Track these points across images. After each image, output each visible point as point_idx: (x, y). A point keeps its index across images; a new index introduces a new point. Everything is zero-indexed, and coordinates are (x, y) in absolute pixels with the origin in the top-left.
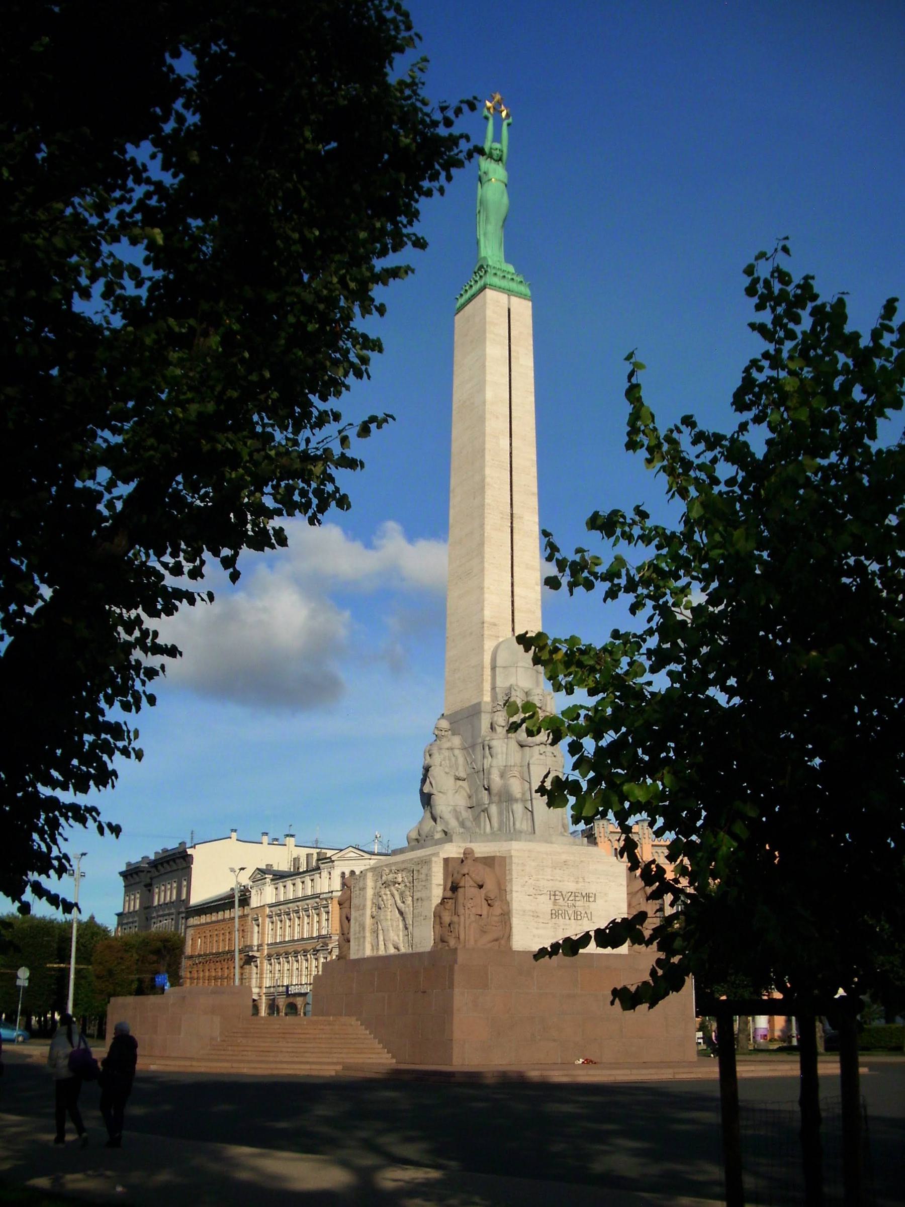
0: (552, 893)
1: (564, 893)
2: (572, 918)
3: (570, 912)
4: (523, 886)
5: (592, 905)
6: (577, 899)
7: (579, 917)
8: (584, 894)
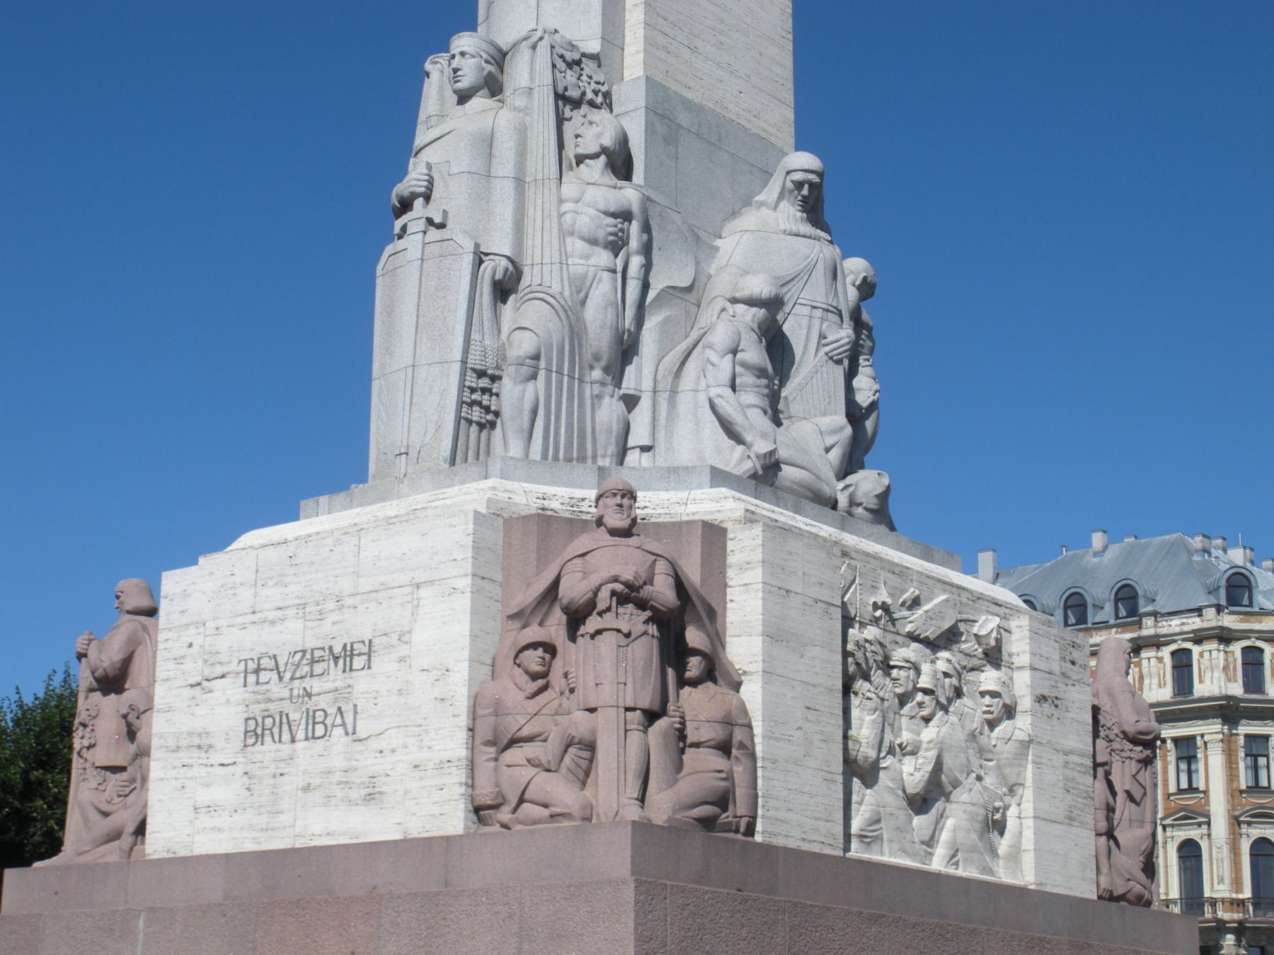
0: (252, 666)
1: (282, 662)
2: (300, 735)
3: (294, 716)
4: (179, 660)
5: (362, 683)
6: (318, 669)
7: (320, 730)
8: (337, 649)
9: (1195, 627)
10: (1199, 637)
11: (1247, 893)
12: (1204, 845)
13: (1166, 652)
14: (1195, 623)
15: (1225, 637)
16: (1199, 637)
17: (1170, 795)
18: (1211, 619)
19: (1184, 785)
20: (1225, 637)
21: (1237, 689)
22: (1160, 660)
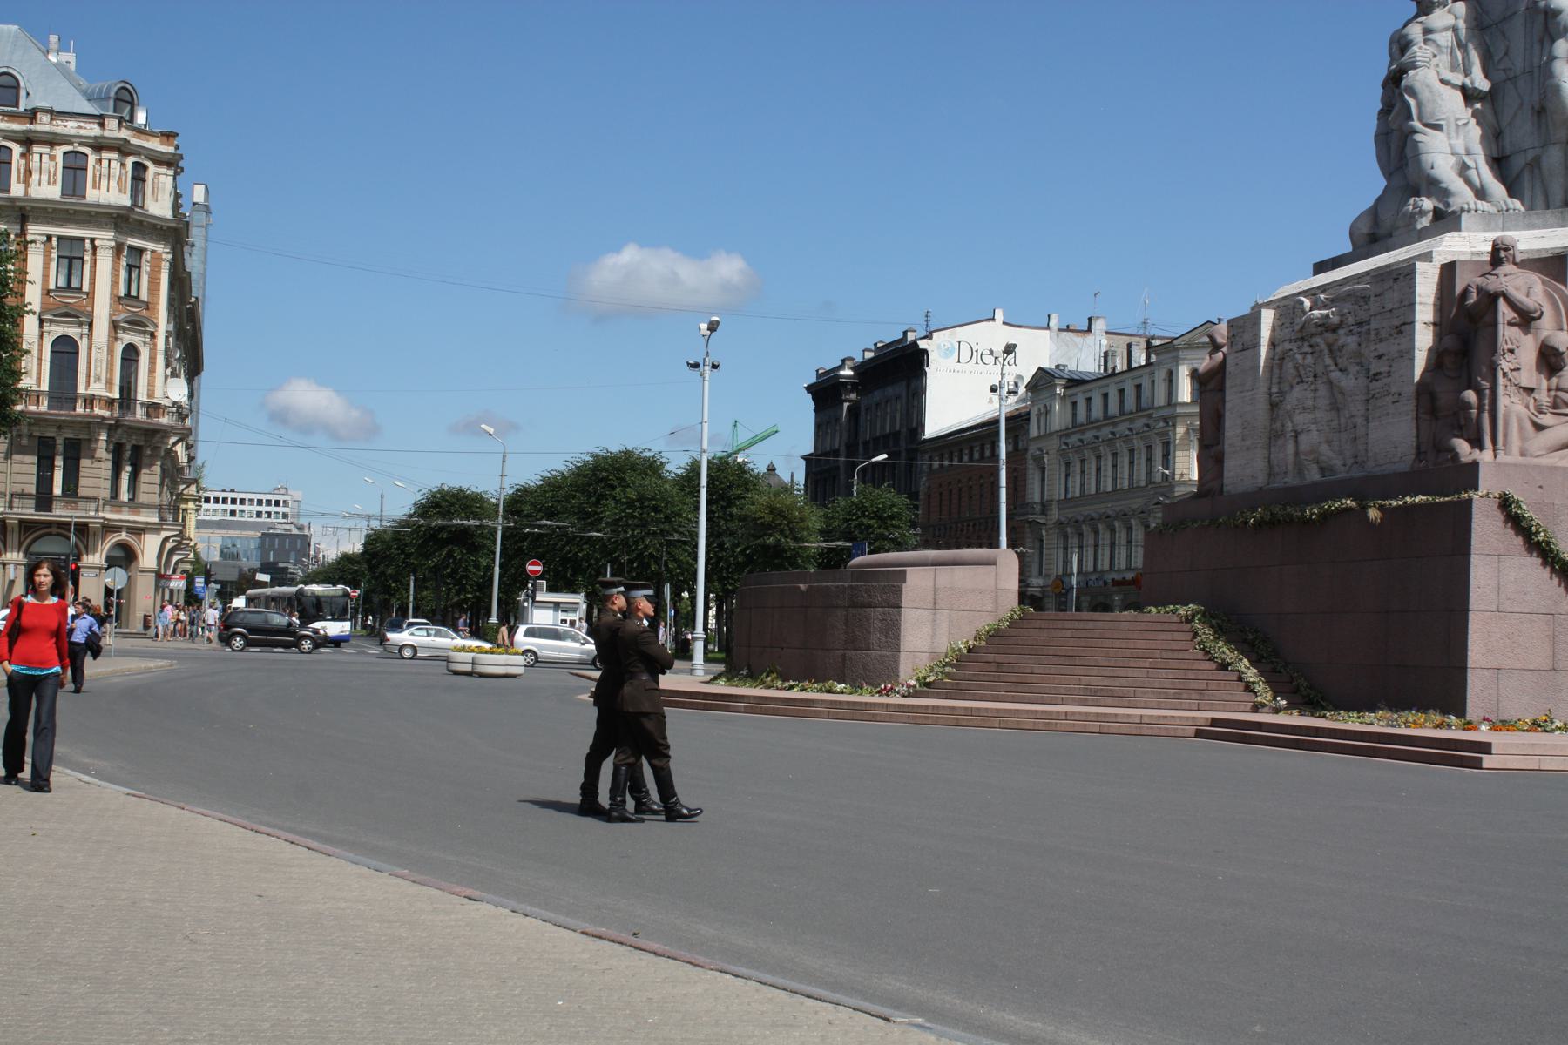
9: (92, 133)
10: (99, 146)
11: (117, 396)
12: (83, 346)
13: (59, 151)
14: (92, 130)
15: (123, 149)
16: (99, 146)
17: (49, 291)
18: (113, 130)
19: (62, 283)
20: (123, 149)
21: (125, 200)
22: (52, 158)
